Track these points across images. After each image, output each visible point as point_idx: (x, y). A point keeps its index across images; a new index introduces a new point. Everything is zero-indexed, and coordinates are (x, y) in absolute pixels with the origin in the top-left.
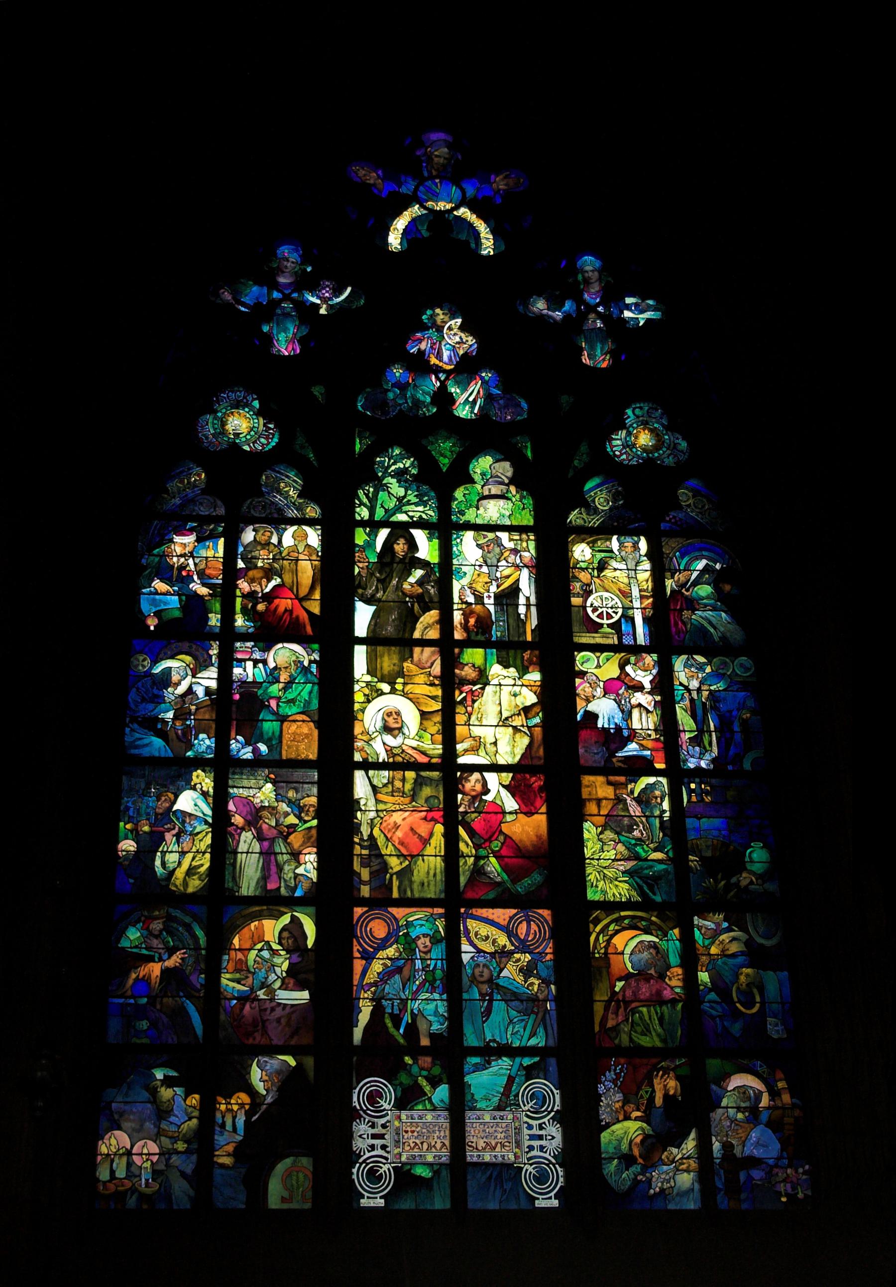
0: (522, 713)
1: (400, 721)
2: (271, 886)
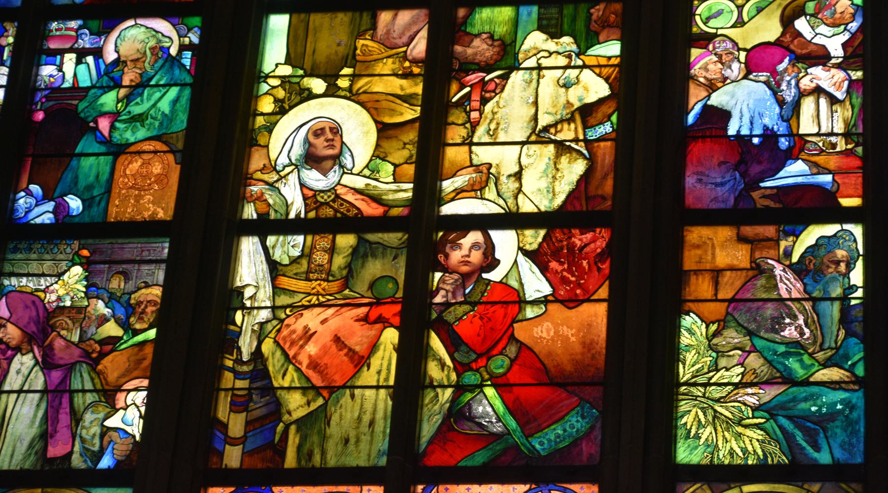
0: (578, 117)
1: (337, 144)
2: (52, 452)
